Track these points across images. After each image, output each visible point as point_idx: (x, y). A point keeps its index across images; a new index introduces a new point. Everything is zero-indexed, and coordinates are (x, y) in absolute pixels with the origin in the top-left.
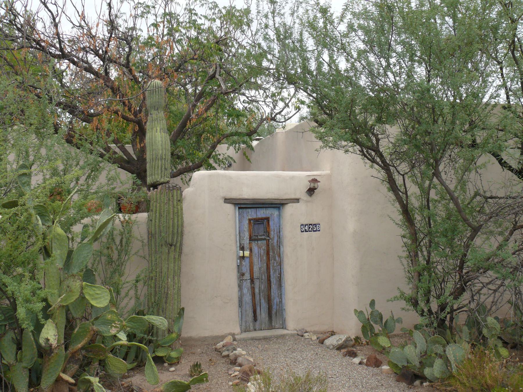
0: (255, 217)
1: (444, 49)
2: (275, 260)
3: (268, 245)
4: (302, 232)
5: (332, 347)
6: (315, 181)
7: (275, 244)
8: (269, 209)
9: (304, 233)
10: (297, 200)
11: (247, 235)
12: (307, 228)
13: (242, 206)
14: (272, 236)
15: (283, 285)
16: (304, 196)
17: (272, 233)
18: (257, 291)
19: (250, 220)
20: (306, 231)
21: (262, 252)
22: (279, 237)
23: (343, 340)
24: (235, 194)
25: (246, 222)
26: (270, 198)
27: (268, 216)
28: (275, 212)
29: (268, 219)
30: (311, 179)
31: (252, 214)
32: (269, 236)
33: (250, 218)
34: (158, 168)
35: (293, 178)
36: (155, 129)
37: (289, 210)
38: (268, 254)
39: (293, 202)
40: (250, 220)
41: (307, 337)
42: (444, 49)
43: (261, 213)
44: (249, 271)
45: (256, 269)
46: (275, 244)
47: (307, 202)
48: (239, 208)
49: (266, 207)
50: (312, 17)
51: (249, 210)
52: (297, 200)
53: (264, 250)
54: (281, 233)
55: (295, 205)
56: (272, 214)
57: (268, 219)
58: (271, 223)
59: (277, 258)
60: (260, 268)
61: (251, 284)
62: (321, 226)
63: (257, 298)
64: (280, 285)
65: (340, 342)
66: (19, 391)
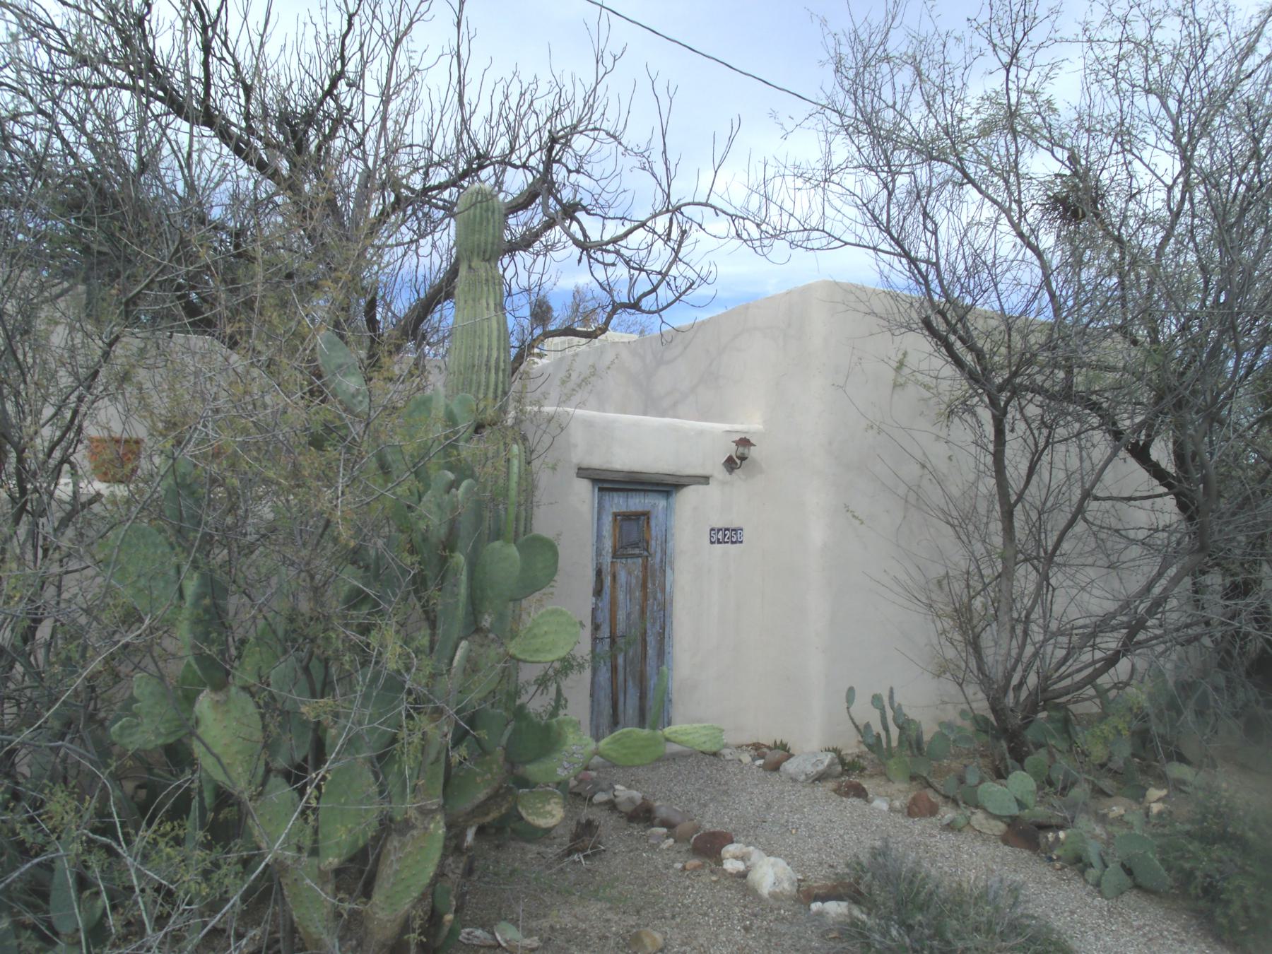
0: (623, 509)
1: (1067, 197)
2: (655, 599)
3: (645, 567)
4: (712, 543)
5: (803, 777)
6: (744, 442)
7: (657, 567)
8: (650, 494)
9: (716, 545)
10: (705, 480)
11: (608, 545)
12: (720, 535)
13: (606, 485)
14: (652, 550)
15: (667, 649)
16: (719, 472)
17: (653, 543)
18: (620, 661)
19: (615, 515)
20: (719, 542)
21: (634, 581)
22: (664, 552)
23: (826, 763)
24: (596, 461)
25: (608, 520)
26: (661, 471)
27: (646, 509)
28: (661, 503)
29: (646, 515)
30: (737, 438)
31: (620, 503)
32: (647, 550)
33: (615, 510)
34: (479, 387)
35: (701, 433)
36: (484, 302)
37: (688, 498)
38: (644, 586)
39: (699, 483)
40: (615, 515)
41: (729, 757)
42: (1067, 197)
43: (636, 503)
44: (608, 622)
45: (621, 615)
46: (657, 567)
47: (724, 483)
48: (601, 489)
49: (645, 491)
50: (1013, 100)
51: (615, 494)
52: (705, 480)
53: (637, 577)
54: (670, 544)
55: (701, 487)
56: (654, 506)
57: (646, 515)
58: (653, 523)
59: (659, 595)
60: (629, 615)
61: (611, 647)
62: (745, 533)
63: (621, 677)
64: (662, 654)
65: (821, 768)
66: (1075, 944)
